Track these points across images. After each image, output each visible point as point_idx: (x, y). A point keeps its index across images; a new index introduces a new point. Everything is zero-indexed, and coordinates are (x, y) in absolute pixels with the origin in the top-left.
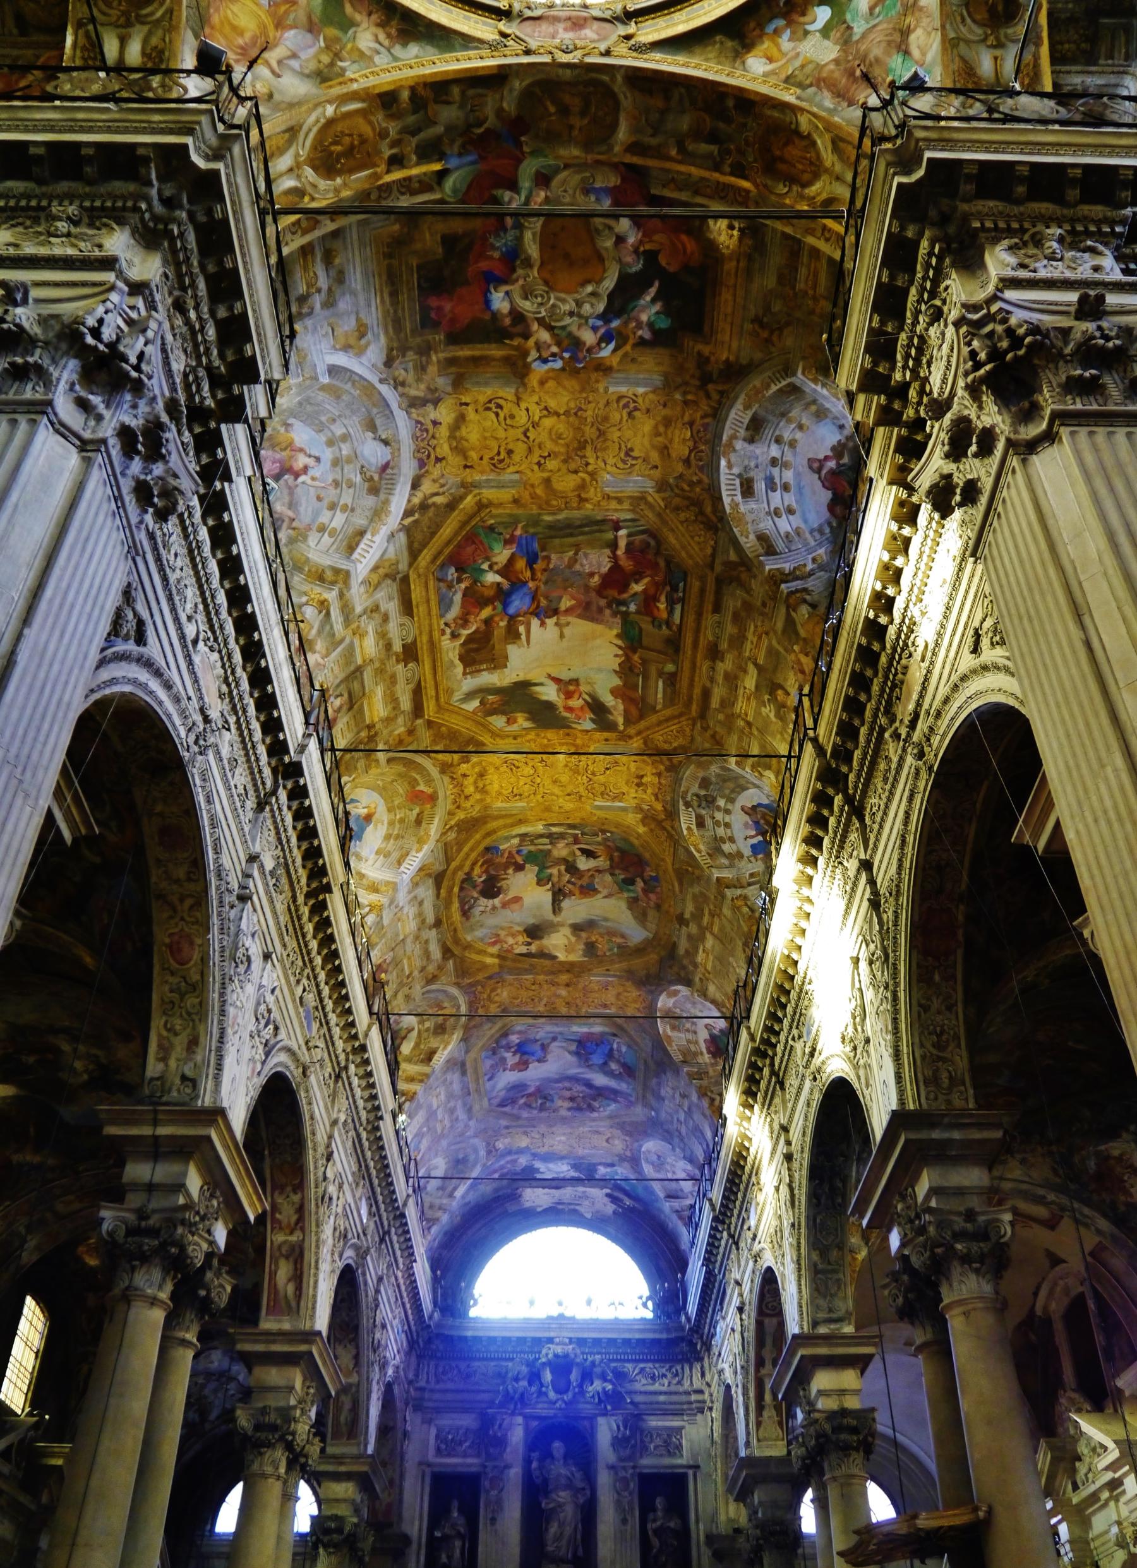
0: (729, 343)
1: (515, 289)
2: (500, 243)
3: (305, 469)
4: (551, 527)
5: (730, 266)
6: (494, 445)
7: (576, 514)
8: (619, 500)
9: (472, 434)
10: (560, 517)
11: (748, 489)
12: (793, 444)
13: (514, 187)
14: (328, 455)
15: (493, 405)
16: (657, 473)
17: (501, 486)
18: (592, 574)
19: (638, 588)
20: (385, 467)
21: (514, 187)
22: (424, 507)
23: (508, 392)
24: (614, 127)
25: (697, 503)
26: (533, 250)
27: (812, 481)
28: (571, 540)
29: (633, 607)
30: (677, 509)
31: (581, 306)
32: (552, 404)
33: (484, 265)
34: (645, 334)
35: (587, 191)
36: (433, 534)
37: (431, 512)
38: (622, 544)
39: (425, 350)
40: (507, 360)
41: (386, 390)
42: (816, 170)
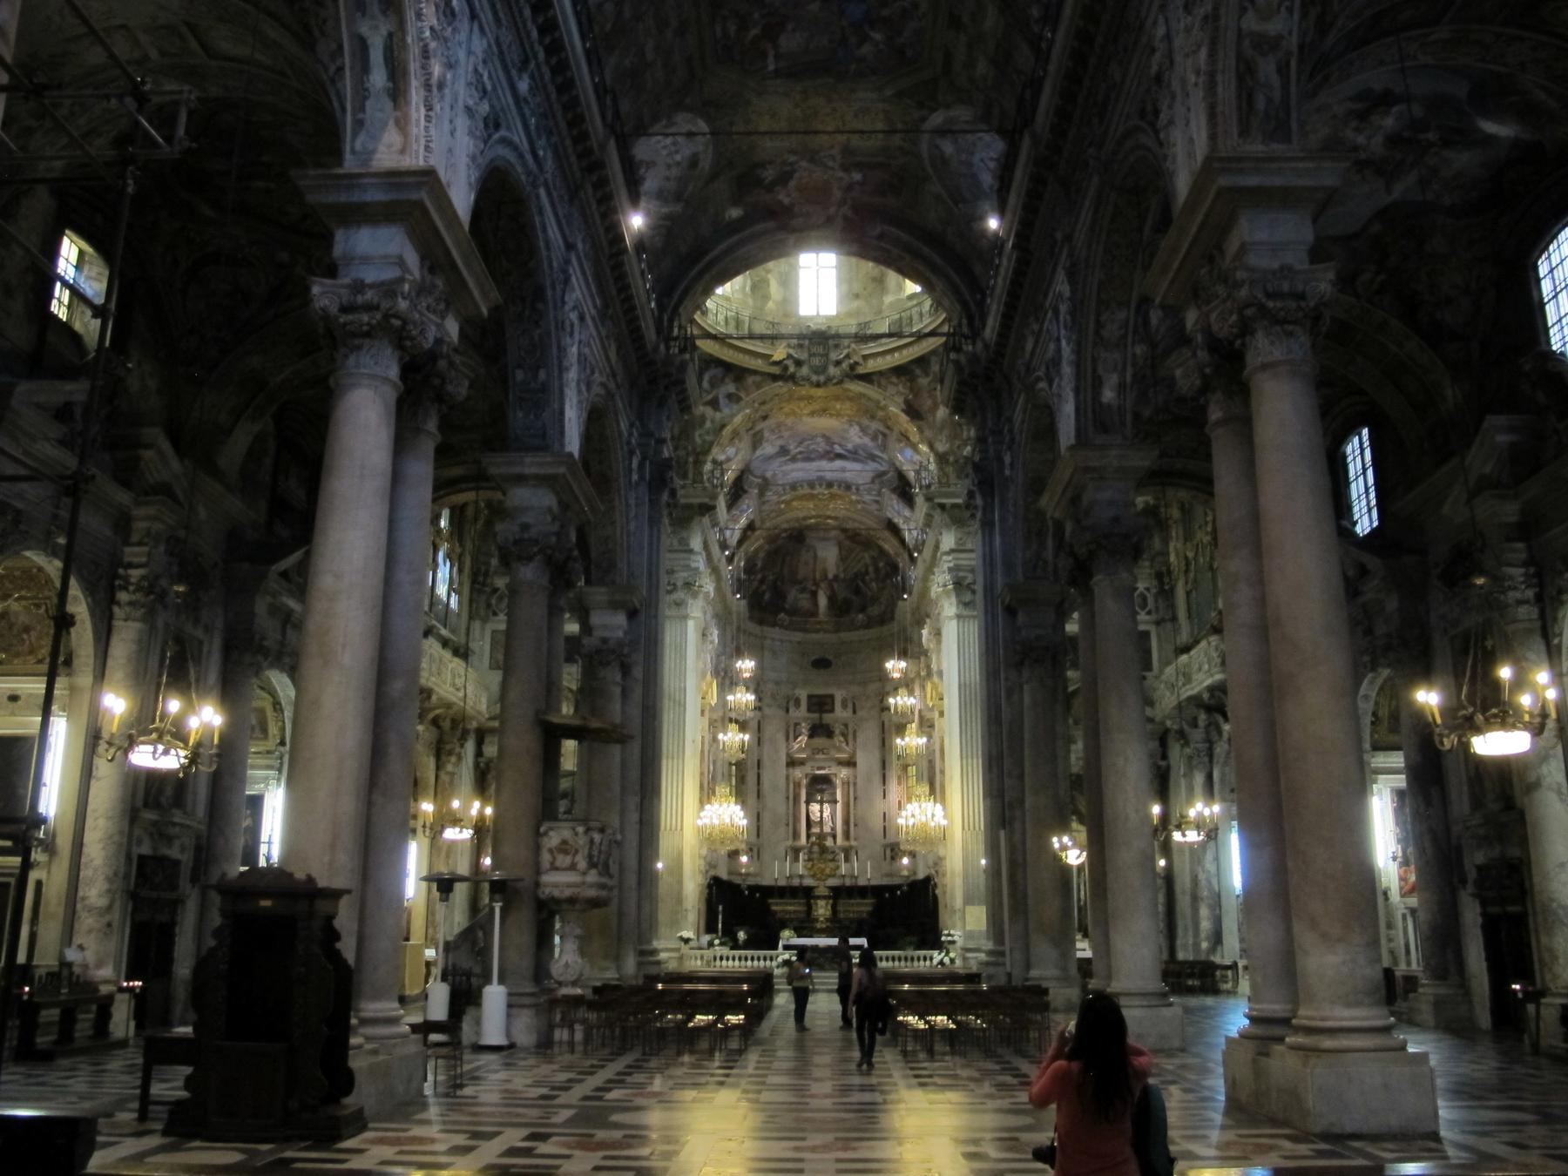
12: (669, 166)
14: (976, 159)
18: (794, 30)
19: (755, 32)
21: (846, 218)
29: (756, 15)
38: (771, 59)
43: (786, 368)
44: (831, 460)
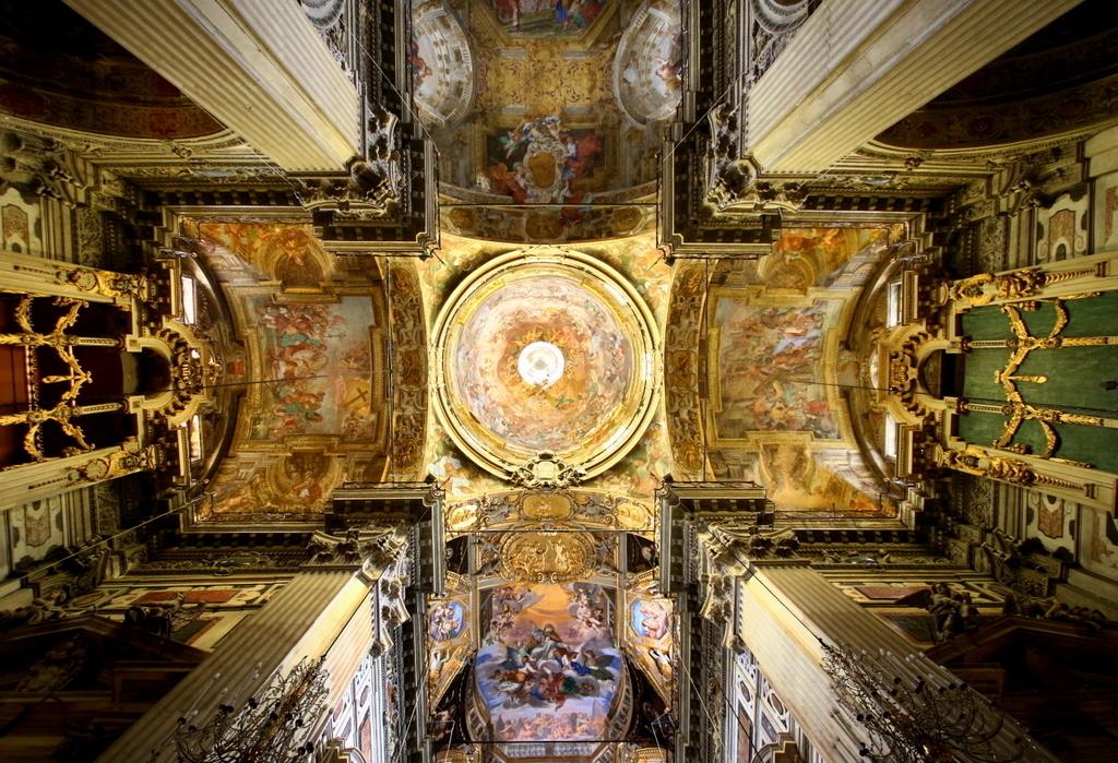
0: (475, 132)
1: (565, 155)
2: (571, 174)
3: (663, 69)
4: (550, 27)
5: (479, 167)
6: (577, 77)
7: (538, 36)
8: (517, 44)
9: (586, 83)
10: (545, 34)
11: (458, 54)
12: (441, 83)
13: (565, 198)
15: (576, 98)
16: (501, 60)
17: (573, 52)
20: (626, 67)
21: (565, 198)
22: (611, 42)
23: (569, 105)
24: (528, 222)
25: (481, 44)
26: (558, 171)
27: (428, 61)
28: (541, 18)
30: (490, 40)
31: (539, 146)
32: (550, 99)
33: (577, 164)
34: (510, 134)
35: (537, 196)
36: (607, 25)
37: (608, 38)
38: (515, 17)
39: (604, 126)
40: (570, 122)
41: (622, 109)
42: (451, 215)
43: (517, 476)
44: (560, 698)
